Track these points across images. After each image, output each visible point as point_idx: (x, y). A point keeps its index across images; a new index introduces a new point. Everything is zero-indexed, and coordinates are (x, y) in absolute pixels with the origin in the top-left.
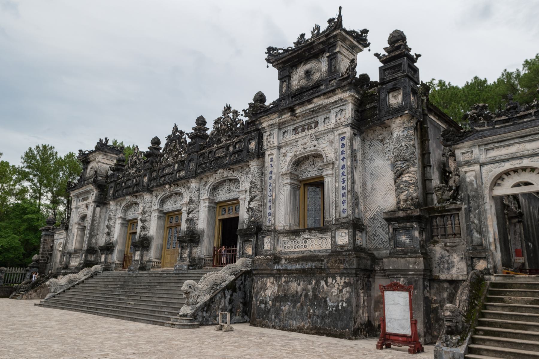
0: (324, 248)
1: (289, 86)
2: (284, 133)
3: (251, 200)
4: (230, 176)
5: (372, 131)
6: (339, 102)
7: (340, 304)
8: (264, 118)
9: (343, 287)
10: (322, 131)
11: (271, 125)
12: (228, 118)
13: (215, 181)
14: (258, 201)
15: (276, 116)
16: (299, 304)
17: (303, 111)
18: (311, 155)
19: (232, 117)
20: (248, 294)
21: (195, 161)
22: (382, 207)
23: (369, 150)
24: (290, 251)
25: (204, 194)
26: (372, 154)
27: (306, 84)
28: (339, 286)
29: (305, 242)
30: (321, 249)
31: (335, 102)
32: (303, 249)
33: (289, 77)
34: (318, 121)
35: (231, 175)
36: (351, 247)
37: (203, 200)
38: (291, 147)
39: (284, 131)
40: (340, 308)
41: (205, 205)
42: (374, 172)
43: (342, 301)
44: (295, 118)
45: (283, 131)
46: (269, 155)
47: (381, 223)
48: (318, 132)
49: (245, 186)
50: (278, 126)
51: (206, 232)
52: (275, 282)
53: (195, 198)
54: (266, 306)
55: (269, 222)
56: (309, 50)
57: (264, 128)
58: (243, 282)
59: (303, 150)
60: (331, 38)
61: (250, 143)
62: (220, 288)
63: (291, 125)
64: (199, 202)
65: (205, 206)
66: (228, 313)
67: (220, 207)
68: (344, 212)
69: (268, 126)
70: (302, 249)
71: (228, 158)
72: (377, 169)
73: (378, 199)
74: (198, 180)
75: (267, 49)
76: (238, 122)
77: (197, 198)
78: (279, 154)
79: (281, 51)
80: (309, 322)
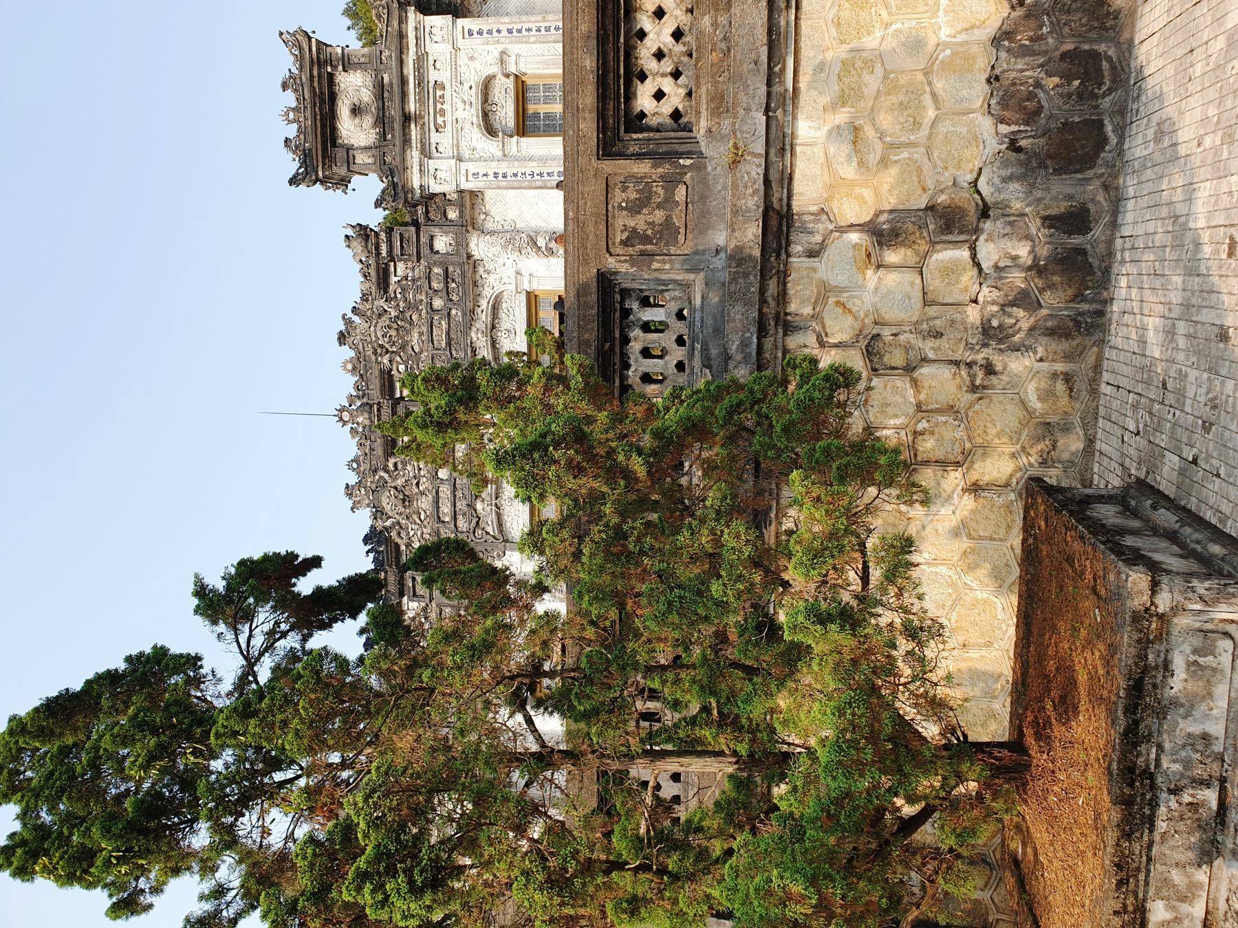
15: (408, 151)
33: (349, 149)
45: (435, 154)
50: (425, 156)
56: (322, 101)
59: (473, 111)
60: (318, 57)
61: (438, 252)
78: (470, 160)
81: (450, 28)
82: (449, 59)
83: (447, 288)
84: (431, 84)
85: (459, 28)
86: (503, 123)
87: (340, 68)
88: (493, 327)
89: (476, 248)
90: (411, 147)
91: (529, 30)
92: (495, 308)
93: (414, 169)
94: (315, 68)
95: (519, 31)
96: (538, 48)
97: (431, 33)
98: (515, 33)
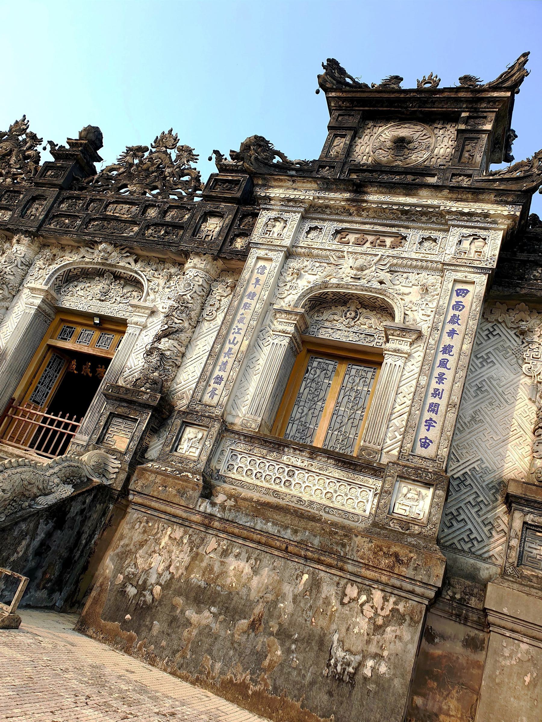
0: (337, 505)
1: (349, 150)
2: (311, 229)
3: (166, 334)
4: (124, 268)
5: (505, 307)
6: (477, 219)
7: (370, 663)
8: (281, 180)
9: (387, 621)
10: (412, 259)
11: (289, 200)
12: (163, 156)
13: (80, 263)
14: (180, 343)
15: (315, 186)
16: (246, 621)
17: (383, 203)
18: (358, 297)
19: (174, 158)
20: (84, 542)
21: (47, 203)
22: (487, 464)
23: (486, 341)
24: (243, 479)
25: (36, 279)
26: (490, 350)
27: (390, 162)
28: (376, 613)
29: (291, 474)
30: (331, 505)
31: (470, 214)
32: (284, 489)
33: (356, 133)
34: (404, 238)
35: (127, 265)
36: (432, 531)
37: (32, 289)
38: (318, 264)
39: (314, 224)
40: (368, 672)
41: (31, 300)
42: (486, 387)
43: (377, 656)
44: (352, 210)
45: (307, 225)
46: (258, 258)
47: (478, 496)
48: (398, 258)
49: (153, 301)
50: (307, 211)
51: (8, 358)
52: (185, 541)
53: (12, 278)
54: (140, 594)
55: (212, 397)
56: (423, 102)
57: (270, 199)
58: (85, 509)
60: (482, 99)
61: (205, 220)
62: (30, 506)
63: (335, 220)
64: (19, 291)
65: (32, 304)
66: (24, 578)
67: (62, 320)
68: (425, 444)
69: (283, 200)
70: (277, 488)
71: (136, 229)
72: (494, 383)
73: (483, 445)
74: (35, 247)
75: (328, 60)
76: (186, 171)
77: (18, 280)
79: (348, 80)
80: (263, 679)
81: (476, 264)
82: (430, 257)
83: (163, 225)
84: (403, 231)
85: (471, 277)
86: (327, 324)
87: (462, 127)
88: (117, 277)
89: (192, 265)
90: (321, 190)
91: (441, 378)
92: (136, 284)
93: (290, 192)
94: (469, 95)
95: (443, 364)
96: (408, 389)
97: (476, 237)
98: (441, 356)
